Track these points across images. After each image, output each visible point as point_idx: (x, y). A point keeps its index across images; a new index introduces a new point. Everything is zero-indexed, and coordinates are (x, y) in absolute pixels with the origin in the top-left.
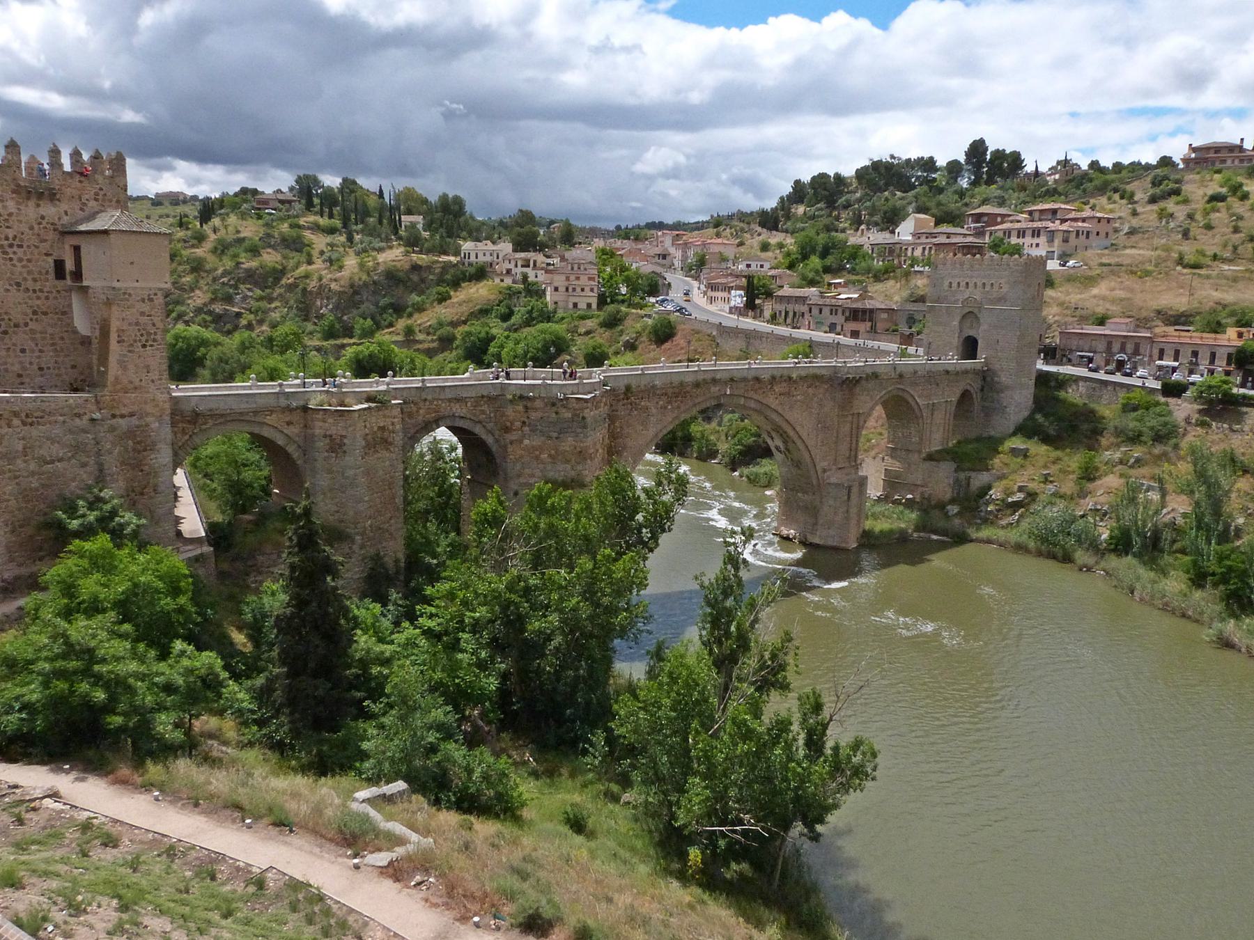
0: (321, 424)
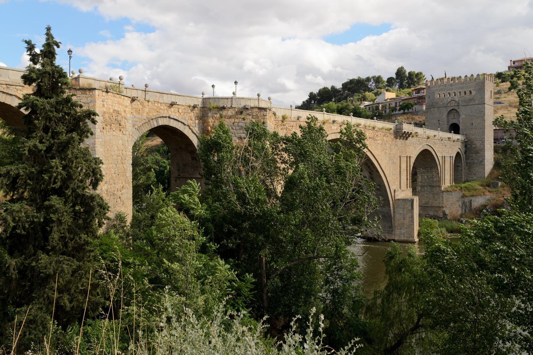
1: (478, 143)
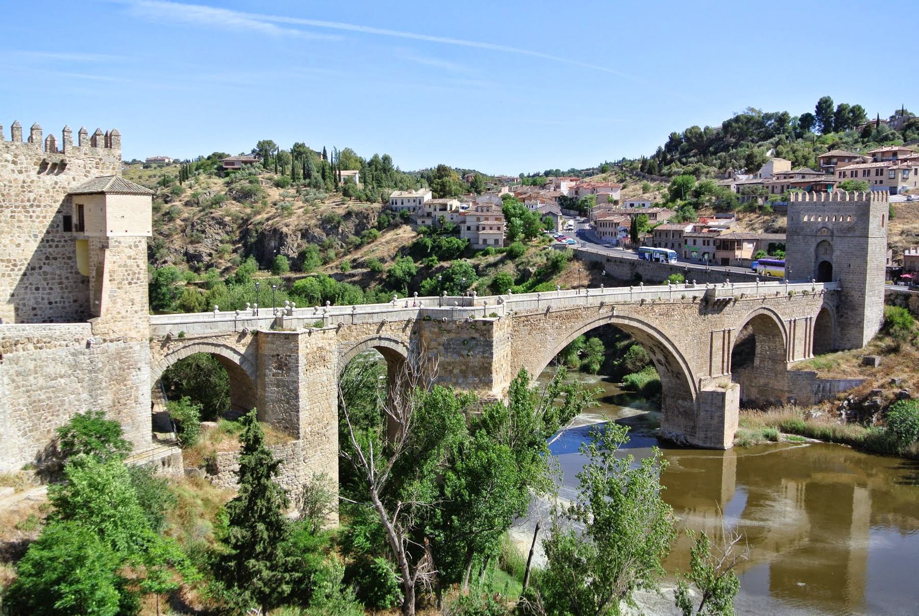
0: (270, 346)
1: (856, 295)
